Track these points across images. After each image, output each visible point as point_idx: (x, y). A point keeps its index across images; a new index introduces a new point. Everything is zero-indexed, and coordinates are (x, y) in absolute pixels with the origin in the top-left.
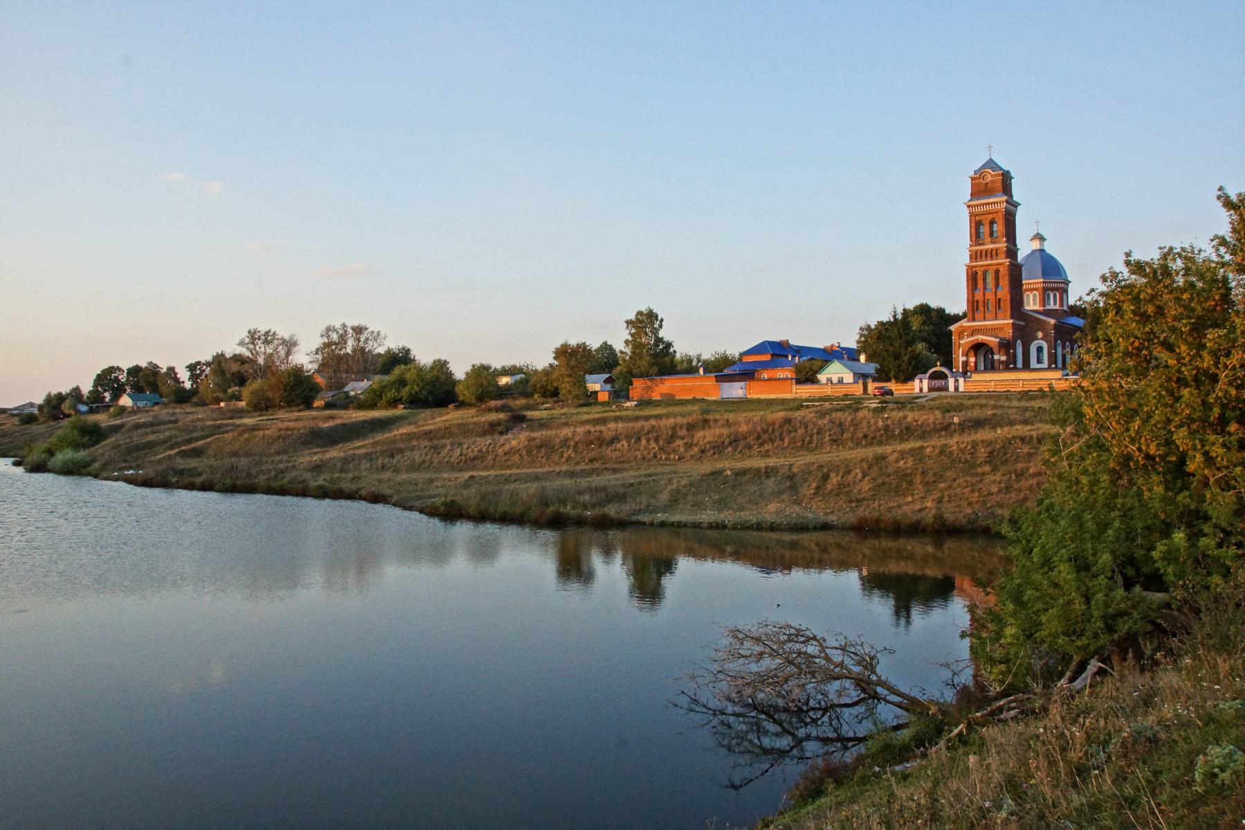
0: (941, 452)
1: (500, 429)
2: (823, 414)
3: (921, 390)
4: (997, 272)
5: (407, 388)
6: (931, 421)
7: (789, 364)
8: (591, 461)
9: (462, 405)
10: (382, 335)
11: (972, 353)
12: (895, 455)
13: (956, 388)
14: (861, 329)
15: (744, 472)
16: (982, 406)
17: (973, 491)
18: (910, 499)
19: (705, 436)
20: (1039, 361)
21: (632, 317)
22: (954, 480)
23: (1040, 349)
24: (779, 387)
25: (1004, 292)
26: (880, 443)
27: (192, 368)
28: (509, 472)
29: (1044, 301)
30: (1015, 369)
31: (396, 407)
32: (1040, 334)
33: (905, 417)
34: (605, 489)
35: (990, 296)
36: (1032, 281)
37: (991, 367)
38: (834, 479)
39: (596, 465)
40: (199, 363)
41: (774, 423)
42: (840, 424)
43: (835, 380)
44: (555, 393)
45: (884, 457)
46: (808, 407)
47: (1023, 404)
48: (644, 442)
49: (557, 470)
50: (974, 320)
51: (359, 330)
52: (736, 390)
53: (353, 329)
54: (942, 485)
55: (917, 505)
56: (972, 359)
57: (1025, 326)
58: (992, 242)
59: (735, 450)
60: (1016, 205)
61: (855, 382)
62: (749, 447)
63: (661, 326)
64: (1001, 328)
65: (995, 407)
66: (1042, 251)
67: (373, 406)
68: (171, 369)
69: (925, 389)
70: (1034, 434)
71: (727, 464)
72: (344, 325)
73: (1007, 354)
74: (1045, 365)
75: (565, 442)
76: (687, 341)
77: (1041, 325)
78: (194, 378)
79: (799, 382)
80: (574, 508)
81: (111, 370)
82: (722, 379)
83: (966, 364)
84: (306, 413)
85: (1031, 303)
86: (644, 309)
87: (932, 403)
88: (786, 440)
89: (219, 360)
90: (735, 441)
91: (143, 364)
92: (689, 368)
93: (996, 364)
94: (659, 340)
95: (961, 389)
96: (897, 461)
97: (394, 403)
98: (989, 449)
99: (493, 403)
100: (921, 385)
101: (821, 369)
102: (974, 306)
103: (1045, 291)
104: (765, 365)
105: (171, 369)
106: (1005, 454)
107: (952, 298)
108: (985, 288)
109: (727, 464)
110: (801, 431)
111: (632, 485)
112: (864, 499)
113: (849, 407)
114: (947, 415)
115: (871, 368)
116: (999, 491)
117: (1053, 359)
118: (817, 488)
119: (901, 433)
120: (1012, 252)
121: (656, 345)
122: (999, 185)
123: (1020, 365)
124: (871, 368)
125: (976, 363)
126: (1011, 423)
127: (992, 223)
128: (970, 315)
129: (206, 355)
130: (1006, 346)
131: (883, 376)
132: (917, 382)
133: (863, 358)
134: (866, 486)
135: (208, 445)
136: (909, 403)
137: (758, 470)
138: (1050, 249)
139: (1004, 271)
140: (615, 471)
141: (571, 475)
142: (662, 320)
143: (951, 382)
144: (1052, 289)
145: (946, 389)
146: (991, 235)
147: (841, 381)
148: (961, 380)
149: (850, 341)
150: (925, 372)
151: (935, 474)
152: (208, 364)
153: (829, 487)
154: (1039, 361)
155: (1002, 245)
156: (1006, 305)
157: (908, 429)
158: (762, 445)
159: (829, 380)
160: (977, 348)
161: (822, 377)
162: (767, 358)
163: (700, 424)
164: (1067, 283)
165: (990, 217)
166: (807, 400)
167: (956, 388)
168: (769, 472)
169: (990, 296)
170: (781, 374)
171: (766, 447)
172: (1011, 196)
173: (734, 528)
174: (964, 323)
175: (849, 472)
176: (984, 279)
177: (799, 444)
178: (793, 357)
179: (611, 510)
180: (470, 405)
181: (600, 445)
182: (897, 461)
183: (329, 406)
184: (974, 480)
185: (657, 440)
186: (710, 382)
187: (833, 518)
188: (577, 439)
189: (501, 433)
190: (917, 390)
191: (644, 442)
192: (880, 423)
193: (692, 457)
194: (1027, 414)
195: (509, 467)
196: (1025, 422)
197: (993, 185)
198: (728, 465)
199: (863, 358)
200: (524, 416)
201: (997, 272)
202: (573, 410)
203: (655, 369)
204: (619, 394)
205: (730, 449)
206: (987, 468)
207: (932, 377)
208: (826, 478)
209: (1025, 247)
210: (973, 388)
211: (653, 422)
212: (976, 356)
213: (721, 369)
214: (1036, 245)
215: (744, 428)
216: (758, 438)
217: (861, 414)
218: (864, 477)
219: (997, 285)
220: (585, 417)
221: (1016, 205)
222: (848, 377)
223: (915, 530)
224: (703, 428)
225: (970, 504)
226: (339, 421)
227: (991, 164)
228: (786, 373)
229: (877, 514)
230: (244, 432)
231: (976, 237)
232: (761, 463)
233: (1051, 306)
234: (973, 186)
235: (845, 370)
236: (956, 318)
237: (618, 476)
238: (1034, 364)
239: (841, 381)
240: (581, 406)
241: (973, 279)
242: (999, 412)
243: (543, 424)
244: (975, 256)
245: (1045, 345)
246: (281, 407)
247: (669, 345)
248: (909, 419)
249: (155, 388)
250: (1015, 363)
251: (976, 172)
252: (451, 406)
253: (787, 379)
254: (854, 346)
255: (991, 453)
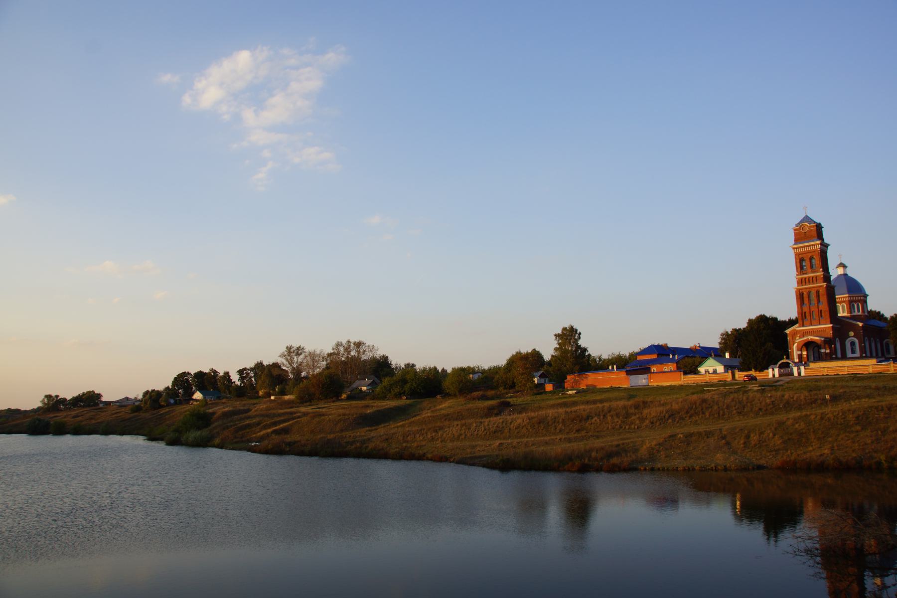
0: (822, 418)
1: (495, 412)
2: (725, 395)
3: (774, 375)
4: (818, 292)
5: (408, 385)
6: (802, 398)
7: (672, 360)
8: (578, 431)
9: (447, 395)
10: (376, 347)
11: (804, 348)
12: (791, 421)
13: (799, 374)
14: (722, 335)
15: (691, 435)
16: (834, 387)
17: (854, 442)
18: (811, 448)
19: (652, 412)
20: (853, 352)
21: (560, 332)
22: (838, 435)
23: (853, 344)
24: (666, 377)
25: (824, 306)
26: (772, 414)
27: (241, 372)
28: (525, 440)
29: (851, 309)
30: (837, 359)
31: (400, 398)
32: (851, 334)
33: (783, 396)
34: (602, 448)
35: (814, 309)
36: (842, 297)
37: (820, 358)
38: (754, 438)
39: (583, 433)
40: (245, 369)
41: (695, 403)
42: (740, 402)
43: (711, 371)
44: (513, 386)
45: (784, 423)
46: (709, 391)
47: (859, 384)
48: (609, 418)
49: (558, 437)
50: (803, 326)
51: (359, 344)
52: (641, 380)
53: (355, 344)
54: (830, 439)
55: (816, 451)
56: (805, 353)
57: (841, 327)
58: (813, 272)
59: (674, 421)
60: (827, 246)
61: (726, 371)
62: (682, 418)
63: (579, 338)
64: (824, 330)
65: (842, 387)
66: (845, 275)
67: (384, 398)
68: (227, 374)
69: (777, 375)
70: (884, 403)
71: (678, 431)
72: (349, 342)
73: (830, 348)
74: (858, 354)
75: (555, 420)
76: (598, 344)
77: (854, 328)
78: (242, 379)
79: (685, 373)
80: (589, 460)
81: (184, 374)
82: (629, 373)
83: (800, 356)
84: (337, 403)
85: (842, 313)
86: (567, 326)
87: (791, 385)
88: (707, 414)
89: (259, 365)
90: (672, 415)
91: (206, 370)
92: (602, 366)
93: (824, 356)
94: (579, 347)
95: (803, 374)
96: (793, 425)
97: (399, 396)
98: (855, 415)
99: (475, 394)
100: (773, 373)
101: (700, 364)
102: (803, 318)
103: (851, 304)
104: (653, 362)
105: (227, 374)
106: (867, 418)
107: (784, 308)
108: (810, 304)
109: (678, 431)
110: (716, 407)
111: (618, 446)
112: (779, 450)
113: (739, 390)
114: (813, 393)
115: (737, 362)
116: (872, 442)
117: (863, 350)
118: (745, 443)
119: (784, 406)
120: (827, 278)
121: (576, 351)
122: (815, 233)
123: (839, 355)
124: (737, 362)
125: (807, 355)
126: (858, 398)
127: (811, 259)
128: (800, 321)
129: (250, 364)
130: (828, 342)
131: (744, 367)
132: (770, 370)
133: (727, 355)
134: (777, 441)
135: (291, 425)
136: (772, 385)
137: (700, 434)
138: (851, 273)
139: (822, 292)
140: (598, 437)
141: (569, 440)
142: (580, 334)
143: (795, 369)
144: (856, 301)
145: (792, 374)
146: (811, 267)
147: (715, 372)
148: (802, 368)
149: (714, 342)
150: (776, 364)
151: (823, 432)
152: (251, 369)
153: (753, 443)
154: (853, 352)
155: (820, 273)
156: (826, 315)
157: (788, 403)
158: (690, 417)
159: (707, 371)
160: (808, 345)
161: (702, 369)
162: (654, 357)
163: (641, 405)
164: (866, 296)
165: (810, 255)
166: (707, 386)
167: (799, 374)
168: (708, 434)
169: (814, 309)
170: (666, 368)
171: (694, 418)
172: (822, 239)
173: (701, 471)
174: (796, 327)
175: (762, 433)
176: (809, 297)
177: (716, 416)
178: (674, 356)
179: (615, 460)
180: (455, 395)
181: (580, 421)
182: (793, 425)
183: (349, 398)
184: (852, 435)
185: (617, 415)
186: (622, 375)
187: (762, 462)
188: (563, 416)
189: (497, 415)
190: (771, 376)
191: (609, 418)
192: (768, 401)
193: (647, 426)
194: (868, 391)
195: (520, 437)
196: (868, 396)
197: (810, 233)
198: (680, 431)
199: (727, 355)
200: (509, 403)
201: (818, 292)
202: (534, 398)
203: (577, 367)
204: (560, 384)
205: (670, 421)
206: (858, 428)
207: (780, 367)
208: (748, 437)
209: (835, 272)
210: (811, 373)
211: (606, 404)
212: (807, 350)
213: (630, 364)
214: (840, 271)
215: (675, 406)
216: (687, 412)
217: (751, 394)
218: (774, 435)
219: (818, 301)
220: (552, 402)
221: (827, 246)
222: (720, 369)
223: (820, 468)
224: (645, 407)
225: (853, 451)
226: (375, 409)
227: (807, 219)
228: (672, 367)
229: (792, 458)
230: (314, 417)
231: (801, 268)
232: (702, 428)
233: (856, 313)
234: (795, 234)
235: (718, 364)
236: (792, 322)
237: (601, 440)
238: (849, 355)
239: (715, 372)
240: (536, 394)
241: (801, 297)
242: (847, 390)
243: (522, 409)
244: (801, 282)
245: (856, 341)
246: (319, 399)
247: (585, 350)
248: (786, 397)
249: (216, 388)
250: (836, 354)
251: (797, 225)
252: (438, 397)
253: (671, 371)
254: (717, 346)
255: (858, 417)
